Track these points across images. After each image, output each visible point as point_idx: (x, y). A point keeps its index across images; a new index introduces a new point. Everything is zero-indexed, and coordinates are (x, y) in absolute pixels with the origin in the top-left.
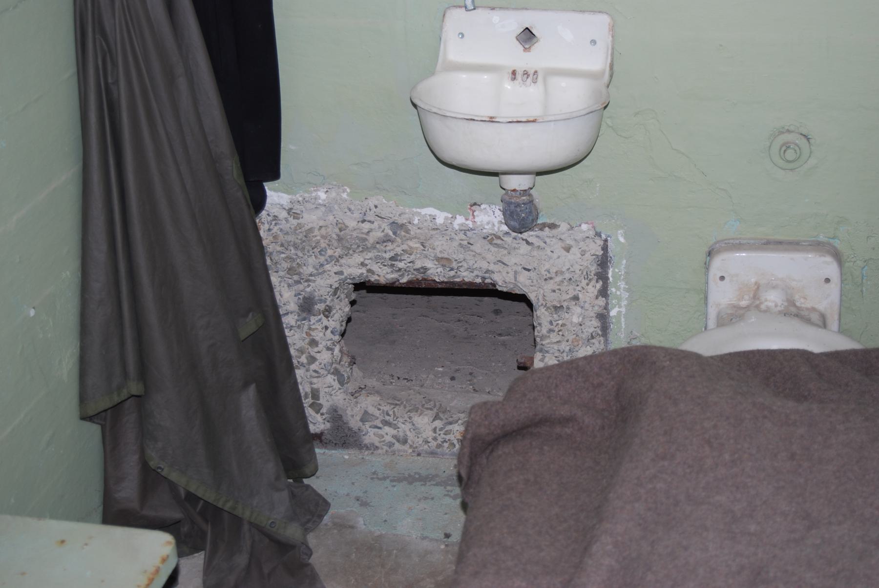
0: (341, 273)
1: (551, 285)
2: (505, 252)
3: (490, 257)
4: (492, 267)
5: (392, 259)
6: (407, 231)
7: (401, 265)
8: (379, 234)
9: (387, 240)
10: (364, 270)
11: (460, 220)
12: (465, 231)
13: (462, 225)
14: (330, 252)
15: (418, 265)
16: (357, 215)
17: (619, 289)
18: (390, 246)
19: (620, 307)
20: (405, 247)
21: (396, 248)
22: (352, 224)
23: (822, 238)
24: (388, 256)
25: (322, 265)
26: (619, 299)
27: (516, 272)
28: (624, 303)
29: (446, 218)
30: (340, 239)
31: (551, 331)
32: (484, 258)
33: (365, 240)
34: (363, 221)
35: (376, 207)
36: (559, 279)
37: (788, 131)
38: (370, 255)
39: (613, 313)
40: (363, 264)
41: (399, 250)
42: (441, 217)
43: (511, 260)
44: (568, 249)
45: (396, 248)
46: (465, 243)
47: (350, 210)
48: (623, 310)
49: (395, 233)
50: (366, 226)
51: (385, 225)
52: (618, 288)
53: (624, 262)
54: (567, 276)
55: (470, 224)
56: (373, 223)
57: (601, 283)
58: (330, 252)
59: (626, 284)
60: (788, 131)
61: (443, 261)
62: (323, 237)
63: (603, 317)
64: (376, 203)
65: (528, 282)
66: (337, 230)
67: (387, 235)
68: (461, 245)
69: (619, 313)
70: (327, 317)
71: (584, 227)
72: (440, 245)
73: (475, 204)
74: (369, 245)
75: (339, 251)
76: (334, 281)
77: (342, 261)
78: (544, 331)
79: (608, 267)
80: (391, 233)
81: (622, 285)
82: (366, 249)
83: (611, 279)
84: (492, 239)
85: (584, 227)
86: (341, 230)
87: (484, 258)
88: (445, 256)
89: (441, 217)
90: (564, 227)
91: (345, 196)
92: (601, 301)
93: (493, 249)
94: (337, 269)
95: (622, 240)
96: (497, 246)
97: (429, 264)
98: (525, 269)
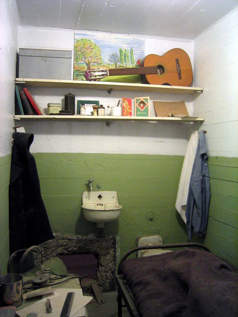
4: (91, 248)
11: (85, 237)
12: (85, 240)
13: (85, 238)
17: (118, 250)
19: (118, 253)
26: (118, 251)
27: (96, 248)
28: (119, 252)
31: (104, 260)
39: (117, 255)
40: (62, 250)
48: (119, 254)
49: (70, 242)
52: (118, 249)
55: (87, 238)
59: (120, 248)
63: (115, 257)
67: (68, 243)
69: (118, 254)
77: (57, 250)
78: (102, 261)
79: (116, 245)
81: (119, 248)
83: (117, 247)
85: (111, 236)
90: (107, 237)
95: (119, 238)
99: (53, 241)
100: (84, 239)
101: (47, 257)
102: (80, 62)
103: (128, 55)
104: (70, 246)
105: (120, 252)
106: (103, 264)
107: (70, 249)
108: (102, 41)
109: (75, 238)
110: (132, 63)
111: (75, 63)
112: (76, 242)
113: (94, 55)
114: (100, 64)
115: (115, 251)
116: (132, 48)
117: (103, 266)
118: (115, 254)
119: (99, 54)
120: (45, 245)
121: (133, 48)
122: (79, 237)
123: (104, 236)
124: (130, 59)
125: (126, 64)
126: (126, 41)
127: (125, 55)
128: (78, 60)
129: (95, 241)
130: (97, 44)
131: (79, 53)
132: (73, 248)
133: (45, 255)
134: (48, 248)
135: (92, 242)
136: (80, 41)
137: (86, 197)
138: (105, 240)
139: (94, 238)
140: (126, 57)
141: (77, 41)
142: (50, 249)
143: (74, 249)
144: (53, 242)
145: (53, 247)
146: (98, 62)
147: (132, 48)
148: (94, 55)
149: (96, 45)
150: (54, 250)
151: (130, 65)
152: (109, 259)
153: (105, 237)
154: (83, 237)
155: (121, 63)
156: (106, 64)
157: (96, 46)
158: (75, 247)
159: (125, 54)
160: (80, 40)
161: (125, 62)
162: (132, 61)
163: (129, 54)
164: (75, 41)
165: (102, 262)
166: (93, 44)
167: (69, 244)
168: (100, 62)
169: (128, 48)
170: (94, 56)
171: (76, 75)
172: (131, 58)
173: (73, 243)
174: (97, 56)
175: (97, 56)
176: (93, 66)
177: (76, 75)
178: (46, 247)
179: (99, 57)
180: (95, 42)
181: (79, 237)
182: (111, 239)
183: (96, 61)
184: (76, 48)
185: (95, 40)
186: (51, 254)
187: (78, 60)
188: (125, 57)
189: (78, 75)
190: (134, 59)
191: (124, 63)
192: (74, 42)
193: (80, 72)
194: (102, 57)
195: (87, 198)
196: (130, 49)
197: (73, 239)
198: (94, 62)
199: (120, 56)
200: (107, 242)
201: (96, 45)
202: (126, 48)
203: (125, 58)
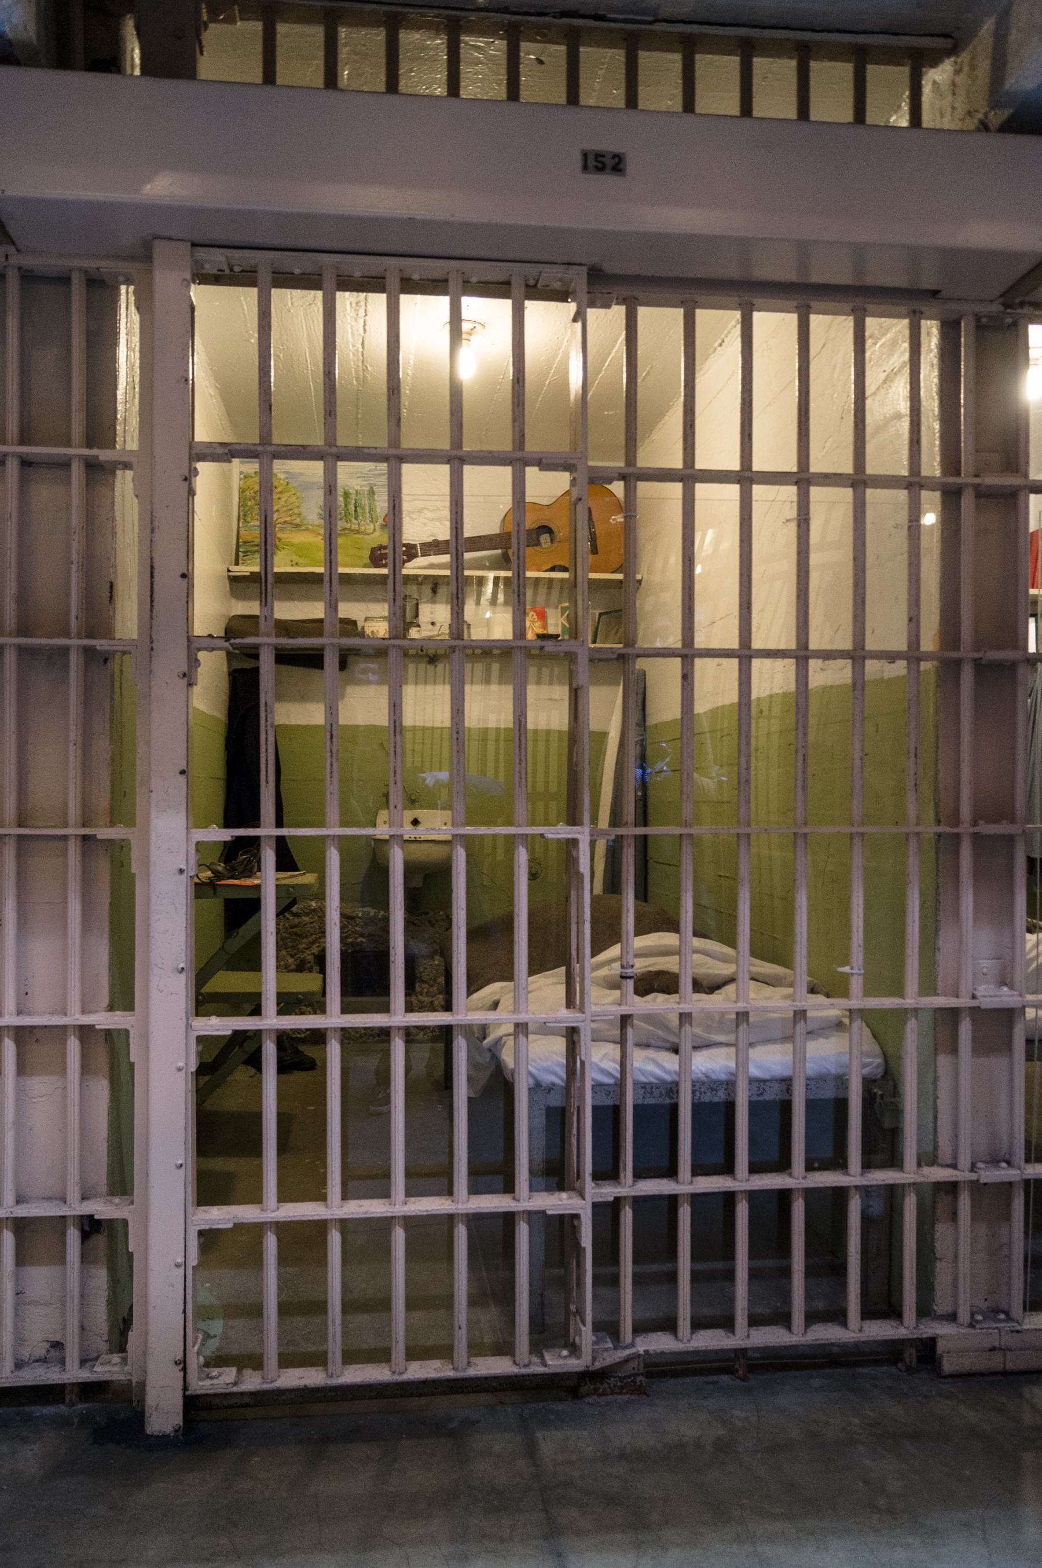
31: (426, 968)
71: (441, 913)
85: (441, 913)
90: (432, 913)
99: (312, 921)
101: (298, 956)
102: (252, 524)
103: (363, 502)
104: (350, 932)
106: (425, 978)
107: (350, 940)
108: (302, 474)
109: (360, 915)
110: (372, 522)
111: (241, 525)
112: (362, 924)
113: (284, 506)
114: (297, 526)
116: (372, 488)
117: (425, 982)
119: (297, 504)
120: (295, 930)
121: (375, 488)
122: (369, 913)
124: (367, 511)
125: (359, 524)
126: (358, 472)
127: (355, 503)
128: (249, 519)
130: (290, 481)
131: (249, 503)
132: (356, 939)
133: (295, 951)
134: (300, 936)
136: (252, 477)
137: (385, 823)
138: (430, 922)
140: (358, 509)
141: (245, 477)
142: (306, 937)
143: (359, 940)
144: (311, 923)
145: (312, 934)
146: (294, 522)
147: (372, 488)
148: (284, 506)
149: (288, 484)
150: (313, 943)
151: (368, 524)
152: (438, 965)
153: (427, 913)
155: (347, 522)
156: (312, 525)
157: (290, 486)
158: (362, 935)
159: (356, 500)
160: (253, 475)
161: (356, 518)
162: (374, 516)
163: (365, 502)
164: (242, 476)
165: (421, 973)
166: (282, 481)
167: (347, 927)
168: (298, 521)
169: (363, 488)
170: (284, 509)
171: (243, 552)
172: (371, 510)
173: (357, 925)
174: (290, 510)
175: (290, 510)
176: (282, 530)
177: (243, 552)
178: (296, 934)
179: (296, 511)
180: (287, 478)
181: (369, 913)
182: (443, 920)
183: (288, 519)
184: (243, 492)
185: (287, 473)
186: (307, 949)
187: (249, 519)
188: (356, 507)
189: (250, 551)
190: (378, 510)
191: (354, 521)
192: (241, 479)
193: (252, 546)
194: (302, 510)
195: (388, 824)
196: (367, 489)
197: (358, 917)
198: (285, 522)
199: (343, 506)
200: (433, 926)
201: (288, 484)
202: (358, 488)
203: (356, 511)
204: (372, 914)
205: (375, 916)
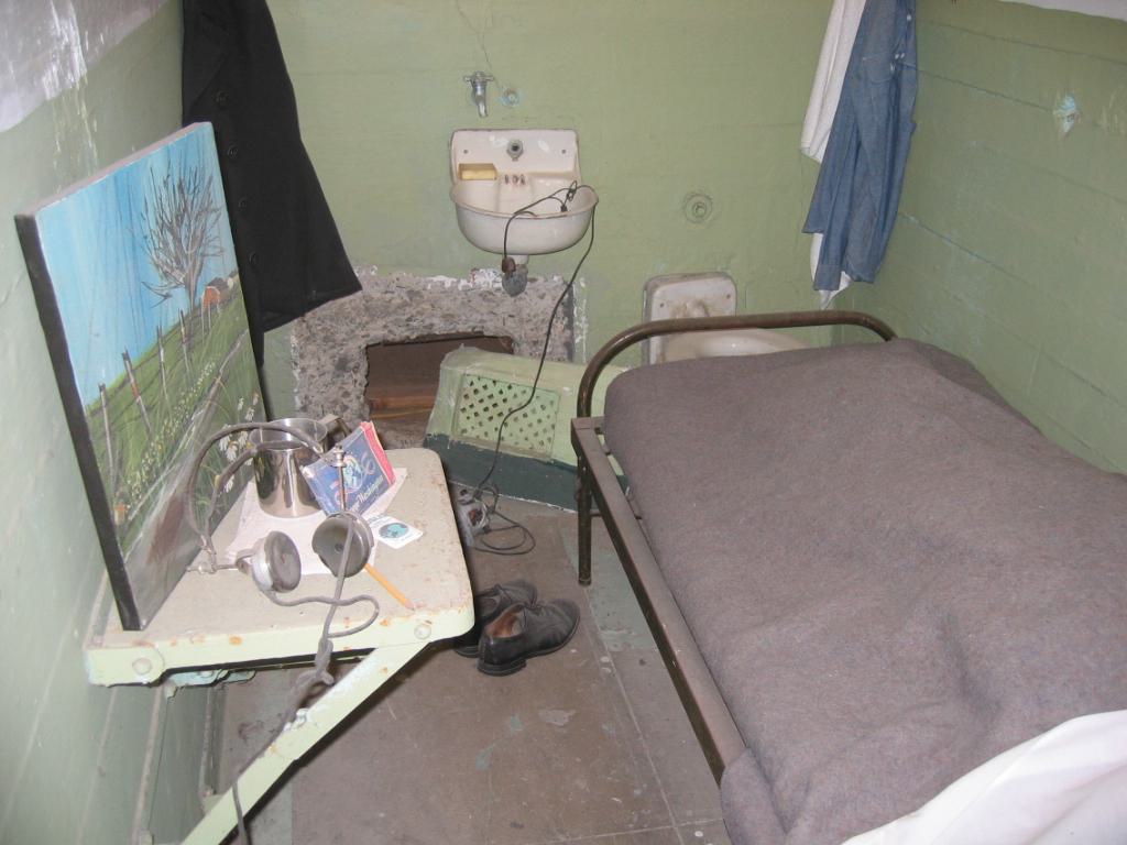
0: (368, 336)
1: (531, 326)
2: (494, 304)
3: (484, 310)
4: (485, 318)
5: (409, 320)
6: (421, 297)
7: (414, 324)
8: (399, 301)
9: (404, 305)
10: (386, 332)
11: (463, 282)
12: (466, 290)
14: (358, 320)
15: (427, 322)
16: (382, 288)
17: (581, 323)
18: (408, 309)
20: (419, 309)
21: (410, 311)
22: (376, 295)
23: (719, 269)
24: (406, 317)
25: (353, 331)
27: (504, 320)
28: (584, 332)
29: (453, 282)
30: (367, 309)
32: (478, 312)
33: (387, 307)
34: (386, 292)
35: (398, 279)
36: (535, 320)
37: (697, 195)
38: (391, 319)
39: (577, 341)
40: (385, 327)
41: (414, 312)
42: (448, 282)
43: (499, 311)
44: (542, 297)
45: (410, 311)
46: (466, 300)
47: (377, 284)
48: (584, 337)
49: (411, 299)
50: (388, 296)
51: (403, 295)
52: (580, 322)
53: (585, 301)
54: (541, 317)
55: (471, 285)
56: (393, 292)
57: (566, 319)
58: (358, 320)
60: (697, 195)
61: (448, 317)
62: (353, 309)
64: (398, 276)
65: (514, 325)
66: (364, 302)
68: (463, 303)
69: (582, 340)
70: (355, 372)
71: (556, 278)
72: (447, 304)
73: (475, 269)
74: (390, 310)
75: (366, 318)
76: (363, 343)
77: (370, 326)
80: (408, 300)
81: (584, 319)
82: (389, 314)
84: (486, 296)
86: (367, 301)
87: (478, 312)
88: (451, 312)
89: (448, 282)
90: (541, 280)
91: (373, 273)
92: (568, 332)
93: (485, 304)
94: (363, 333)
95: (583, 285)
96: (489, 300)
97: (436, 321)
98: (511, 316)
100: (460, 288)
105: (590, 330)
115: (570, 326)
118: (572, 337)
123: (529, 276)
129: (499, 294)
135: (491, 297)
139: (497, 285)
154: (459, 281)
204: (448, 285)
205: (453, 288)
